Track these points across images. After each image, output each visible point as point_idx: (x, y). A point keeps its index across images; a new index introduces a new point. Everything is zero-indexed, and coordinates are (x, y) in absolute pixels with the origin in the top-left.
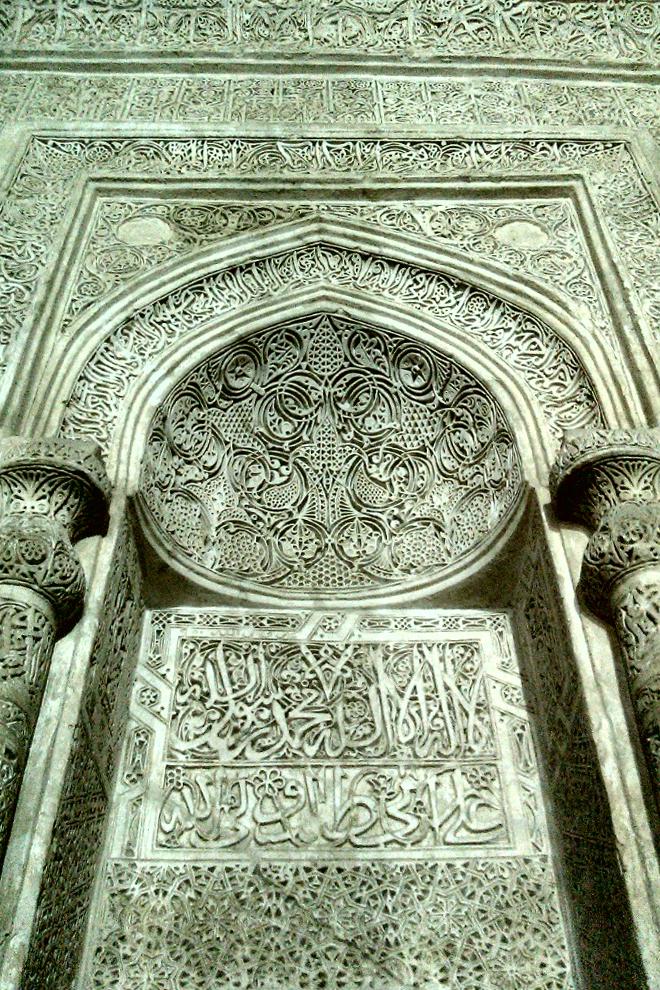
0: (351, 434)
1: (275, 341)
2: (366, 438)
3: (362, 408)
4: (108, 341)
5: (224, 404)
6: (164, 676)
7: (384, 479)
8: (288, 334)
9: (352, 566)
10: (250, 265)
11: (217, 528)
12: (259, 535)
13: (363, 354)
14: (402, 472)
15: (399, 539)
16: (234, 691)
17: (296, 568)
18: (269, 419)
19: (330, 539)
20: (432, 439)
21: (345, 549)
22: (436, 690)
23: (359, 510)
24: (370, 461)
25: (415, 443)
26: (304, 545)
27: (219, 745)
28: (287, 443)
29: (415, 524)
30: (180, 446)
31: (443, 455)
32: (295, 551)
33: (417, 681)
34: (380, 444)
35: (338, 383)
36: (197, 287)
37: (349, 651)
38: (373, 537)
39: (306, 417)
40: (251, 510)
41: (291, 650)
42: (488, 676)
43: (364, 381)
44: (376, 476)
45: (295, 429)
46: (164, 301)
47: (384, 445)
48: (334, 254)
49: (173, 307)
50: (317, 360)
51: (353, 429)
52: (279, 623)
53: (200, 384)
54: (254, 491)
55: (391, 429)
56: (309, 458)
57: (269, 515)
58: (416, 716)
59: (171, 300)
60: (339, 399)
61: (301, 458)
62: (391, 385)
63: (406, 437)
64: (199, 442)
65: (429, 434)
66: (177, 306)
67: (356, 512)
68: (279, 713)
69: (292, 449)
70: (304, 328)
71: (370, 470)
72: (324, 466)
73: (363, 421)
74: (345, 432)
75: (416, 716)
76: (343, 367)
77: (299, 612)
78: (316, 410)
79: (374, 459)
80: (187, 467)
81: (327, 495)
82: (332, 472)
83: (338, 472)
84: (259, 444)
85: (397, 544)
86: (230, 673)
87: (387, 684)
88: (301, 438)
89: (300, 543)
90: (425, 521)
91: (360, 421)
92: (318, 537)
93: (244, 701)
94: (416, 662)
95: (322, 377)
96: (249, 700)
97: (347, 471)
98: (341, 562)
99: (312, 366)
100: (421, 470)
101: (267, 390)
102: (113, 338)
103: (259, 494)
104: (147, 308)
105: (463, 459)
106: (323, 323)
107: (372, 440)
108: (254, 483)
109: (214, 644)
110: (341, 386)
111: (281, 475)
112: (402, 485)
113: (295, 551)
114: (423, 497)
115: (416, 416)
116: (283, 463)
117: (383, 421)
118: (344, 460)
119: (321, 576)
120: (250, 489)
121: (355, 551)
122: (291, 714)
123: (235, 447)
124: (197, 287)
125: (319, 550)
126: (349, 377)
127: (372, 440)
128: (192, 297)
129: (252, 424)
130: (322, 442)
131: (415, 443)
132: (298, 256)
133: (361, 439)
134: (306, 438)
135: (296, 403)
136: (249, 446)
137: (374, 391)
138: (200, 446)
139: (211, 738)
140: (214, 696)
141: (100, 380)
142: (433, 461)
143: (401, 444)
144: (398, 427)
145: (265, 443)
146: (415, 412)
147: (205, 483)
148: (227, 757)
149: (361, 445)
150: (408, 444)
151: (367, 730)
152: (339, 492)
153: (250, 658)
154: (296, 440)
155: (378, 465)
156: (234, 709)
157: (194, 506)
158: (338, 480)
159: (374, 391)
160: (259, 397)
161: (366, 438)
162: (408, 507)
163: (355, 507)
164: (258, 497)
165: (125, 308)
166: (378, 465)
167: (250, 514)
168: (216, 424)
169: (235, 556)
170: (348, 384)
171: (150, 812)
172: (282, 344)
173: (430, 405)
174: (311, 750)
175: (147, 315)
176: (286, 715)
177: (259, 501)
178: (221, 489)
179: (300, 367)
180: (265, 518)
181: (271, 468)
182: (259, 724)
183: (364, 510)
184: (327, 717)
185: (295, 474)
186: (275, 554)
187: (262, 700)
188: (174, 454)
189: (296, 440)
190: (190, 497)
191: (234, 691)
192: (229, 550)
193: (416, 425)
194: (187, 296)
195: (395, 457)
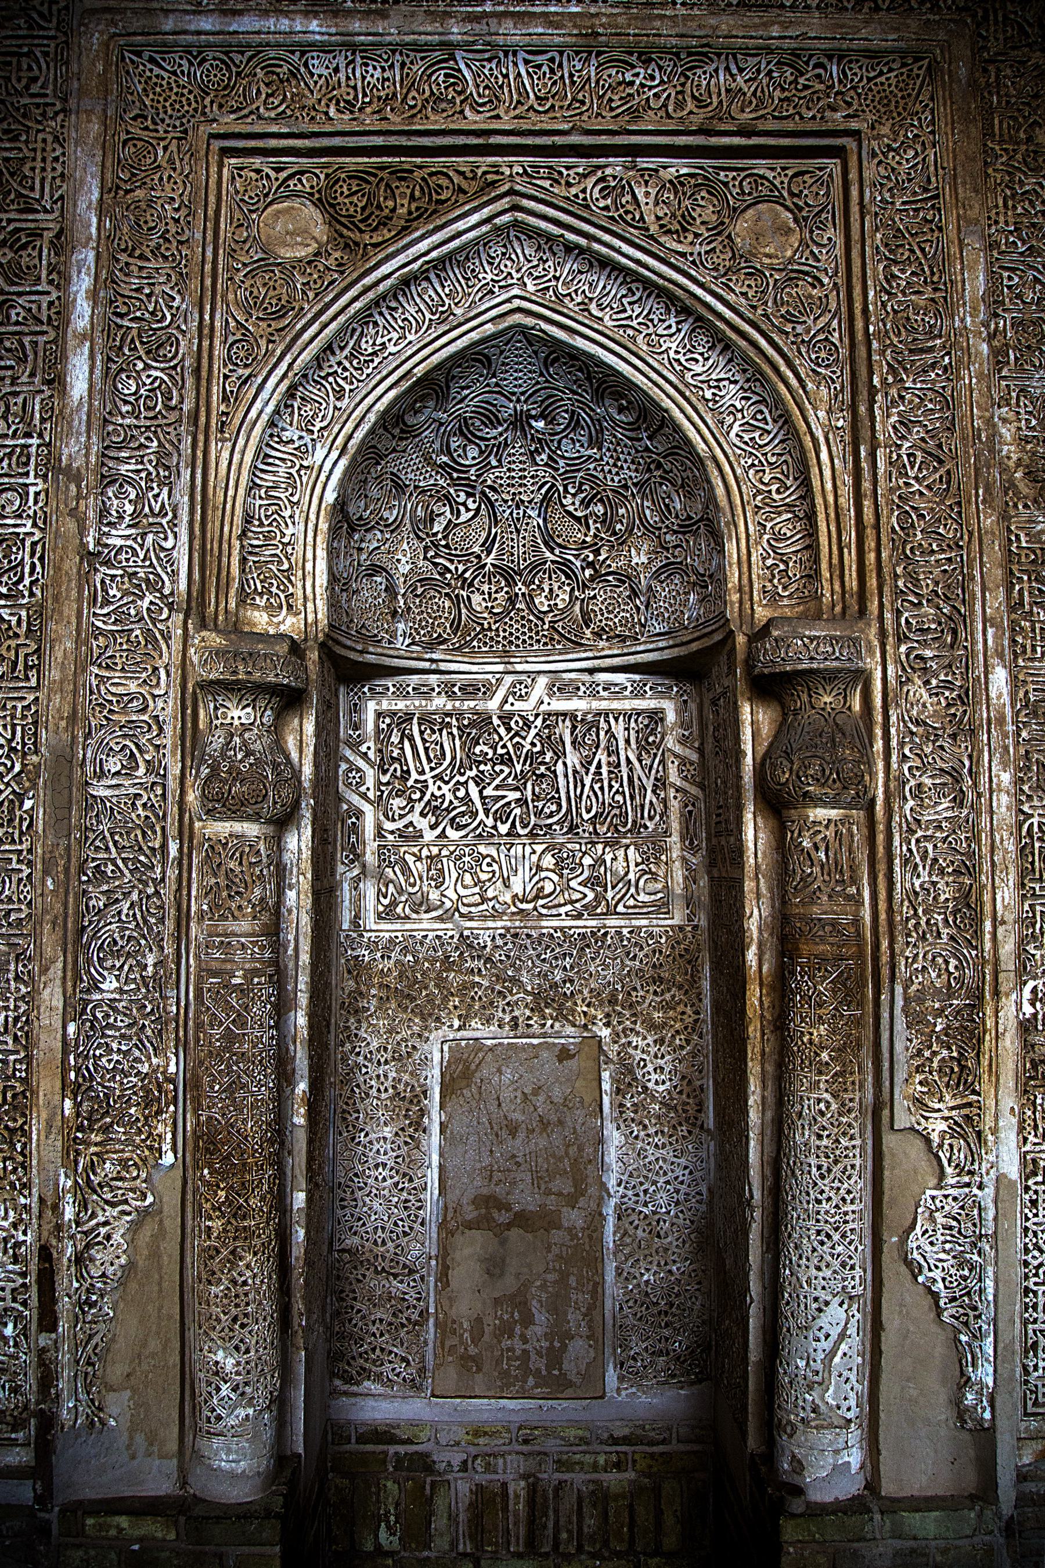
2: (561, 463)
6: (366, 754)
7: (579, 514)
16: (432, 769)
17: (486, 626)
18: (453, 446)
22: (619, 765)
24: (566, 491)
26: (494, 596)
27: (422, 824)
32: (484, 604)
33: (602, 756)
34: (578, 471)
35: (531, 400)
37: (539, 722)
41: (483, 721)
42: (669, 750)
43: (562, 399)
44: (571, 508)
47: (581, 474)
48: (530, 238)
52: (470, 690)
54: (440, 536)
58: (599, 793)
67: (548, 554)
68: (474, 791)
71: (564, 501)
75: (599, 793)
77: (489, 676)
86: (426, 749)
87: (572, 758)
92: (508, 585)
93: (442, 779)
94: (602, 733)
96: (447, 779)
103: (445, 537)
107: (568, 465)
109: (408, 717)
113: (484, 604)
119: (511, 634)
120: (435, 534)
122: (485, 793)
127: (568, 465)
135: (483, 423)
136: (432, 482)
139: (415, 817)
140: (414, 776)
148: (429, 836)
151: (554, 808)
153: (445, 732)
155: (574, 495)
156: (432, 788)
161: (561, 463)
163: (546, 543)
166: (574, 495)
170: (542, 402)
171: (369, 889)
174: (504, 829)
176: (481, 792)
180: (452, 568)
182: (456, 803)
184: (517, 795)
187: (458, 778)
191: (432, 769)
195: (592, 488)
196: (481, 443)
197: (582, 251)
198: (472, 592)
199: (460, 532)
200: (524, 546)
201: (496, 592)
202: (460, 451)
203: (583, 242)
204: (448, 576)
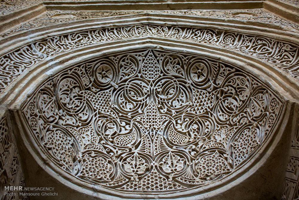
0: (166, 110)
7: (184, 131)
9: (168, 178)
11: (83, 153)
12: (110, 160)
14: (195, 126)
15: (197, 162)
17: (132, 179)
19: (154, 163)
20: (211, 107)
21: (164, 169)
23: (171, 147)
24: (177, 123)
25: (202, 111)
26: (138, 166)
28: (130, 114)
29: (206, 152)
30: (65, 105)
31: (219, 114)
34: (182, 114)
38: (181, 161)
40: (106, 146)
44: (181, 130)
45: (135, 107)
47: (184, 114)
51: (166, 107)
54: (109, 136)
55: (187, 106)
56: (142, 122)
57: (117, 149)
61: (137, 122)
63: (196, 108)
64: (77, 106)
65: (209, 105)
67: (169, 149)
69: (132, 117)
71: (176, 127)
72: (150, 125)
73: (172, 103)
74: (162, 109)
79: (179, 122)
80: (68, 117)
82: (155, 128)
83: (159, 129)
85: (196, 164)
88: (138, 112)
89: (136, 166)
90: (212, 150)
91: (170, 103)
97: (163, 128)
98: (161, 176)
103: (113, 138)
105: (231, 113)
108: (110, 132)
111: (126, 130)
112: (196, 133)
113: (132, 169)
114: (209, 138)
115: (201, 97)
116: (127, 124)
117: (183, 102)
118: (161, 123)
121: (170, 169)
123: (99, 113)
125: (147, 170)
127: (177, 112)
131: (202, 111)
133: (171, 111)
134: (140, 112)
136: (108, 113)
142: (213, 118)
143: (194, 113)
144: (191, 104)
145: (118, 114)
146: (200, 95)
147: (79, 128)
149: (171, 115)
150: (198, 112)
154: (135, 113)
155: (181, 124)
157: (69, 138)
158: (158, 132)
161: (173, 111)
162: (200, 144)
164: (111, 140)
166: (181, 124)
167: (105, 148)
168: (89, 99)
169: (93, 170)
173: (209, 90)
177: (112, 142)
178: (89, 133)
180: (115, 151)
181: (120, 126)
183: (174, 147)
185: (134, 129)
186: (119, 170)
188: (59, 108)
189: (135, 113)
190: (67, 133)
192: (89, 166)
193: (201, 102)
195: (190, 120)
198: (126, 163)
199: (122, 137)
200: (156, 146)
201: (140, 165)
202: (124, 104)
204: (112, 154)
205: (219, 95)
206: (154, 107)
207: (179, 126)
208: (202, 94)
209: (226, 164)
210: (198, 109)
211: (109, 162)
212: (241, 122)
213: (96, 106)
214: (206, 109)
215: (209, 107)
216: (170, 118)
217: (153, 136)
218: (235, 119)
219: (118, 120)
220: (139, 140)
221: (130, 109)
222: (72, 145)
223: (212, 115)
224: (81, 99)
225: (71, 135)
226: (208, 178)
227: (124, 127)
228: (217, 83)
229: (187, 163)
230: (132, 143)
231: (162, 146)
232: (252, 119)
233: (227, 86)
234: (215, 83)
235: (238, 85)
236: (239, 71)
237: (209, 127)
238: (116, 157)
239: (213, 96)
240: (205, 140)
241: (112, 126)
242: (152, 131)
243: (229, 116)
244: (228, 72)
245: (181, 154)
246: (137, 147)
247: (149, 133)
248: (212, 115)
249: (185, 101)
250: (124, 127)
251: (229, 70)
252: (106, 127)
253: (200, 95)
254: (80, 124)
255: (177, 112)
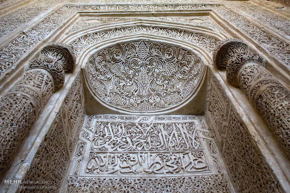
0: (151, 74)
1: (127, 47)
3: (154, 66)
4: (79, 39)
5: (112, 62)
8: (131, 45)
10: (121, 29)
11: (110, 93)
13: (154, 51)
14: (167, 82)
15: (166, 98)
17: (134, 105)
18: (126, 69)
20: (175, 72)
23: (154, 92)
24: (157, 80)
28: (131, 76)
30: (99, 69)
34: (160, 76)
36: (106, 32)
39: (137, 69)
44: (159, 84)
46: (96, 33)
47: (161, 76)
48: (145, 28)
49: (98, 35)
50: (140, 53)
51: (151, 72)
53: (106, 54)
55: (163, 71)
57: (126, 92)
59: (98, 34)
60: (147, 64)
61: (136, 80)
62: (162, 59)
63: (167, 73)
64: (105, 71)
65: (174, 70)
66: (100, 35)
69: (133, 77)
70: (136, 44)
74: (149, 73)
76: (148, 56)
78: (140, 67)
79: (158, 80)
80: (101, 75)
81: (144, 89)
82: (145, 83)
83: (147, 83)
84: (123, 75)
88: (136, 75)
89: (136, 100)
90: (174, 92)
91: (153, 70)
95: (142, 58)
99: (139, 55)
100: (172, 80)
101: (125, 61)
102: (81, 39)
104: (91, 34)
105: (185, 74)
106: (142, 43)
108: (122, 84)
110: (148, 61)
111: (130, 83)
112: (167, 85)
114: (173, 87)
115: (170, 66)
116: (130, 81)
117: (160, 69)
118: (149, 80)
123: (116, 75)
124: (106, 32)
126: (150, 58)
127: (157, 75)
128: (104, 34)
129: (121, 70)
130: (142, 76)
132: (135, 28)
134: (137, 75)
136: (120, 75)
137: (157, 62)
138: (105, 72)
141: (76, 47)
142: (176, 77)
143: (166, 75)
144: (165, 70)
145: (125, 75)
146: (170, 65)
149: (154, 76)
150: (168, 74)
152: (147, 88)
154: (134, 75)
155: (159, 81)
157: (102, 85)
158: (147, 85)
159: (157, 62)
160: (123, 63)
161: (155, 74)
164: (122, 88)
165: (85, 33)
166: (159, 81)
167: (120, 91)
168: (110, 67)
170: (149, 60)
172: (130, 48)
173: (174, 62)
175: (91, 36)
177: (123, 89)
178: (111, 84)
179: (135, 55)
180: (125, 93)
188: (97, 71)
189: (134, 75)
193: (170, 69)
194: (103, 34)
196: (134, 70)
197: (156, 27)
199: (128, 87)
202: (128, 71)
203: (157, 25)
204: (123, 94)
205: (179, 65)
206: (145, 72)
207: (158, 82)
208: (171, 65)
209: (180, 97)
210: (168, 73)
211: (122, 98)
212: (189, 78)
213: (114, 71)
214: (173, 73)
215: (174, 72)
216: (153, 78)
217: (144, 87)
218: (186, 77)
219: (126, 79)
220: (137, 88)
221: (132, 73)
222: (104, 88)
223: (175, 75)
224: (106, 67)
225: (103, 84)
226: (171, 104)
227: (129, 82)
228: (179, 59)
229: (162, 98)
230: (134, 89)
231: (149, 91)
232: (194, 76)
233: (183, 60)
234: (177, 59)
235: (189, 59)
236: (189, 52)
237: (174, 82)
238: (125, 96)
239: (176, 66)
240: (171, 88)
241: (123, 82)
242: (144, 84)
243: (184, 75)
244: (184, 53)
245: (159, 95)
246: (136, 92)
247: (142, 85)
248: (175, 75)
249: (161, 69)
250: (129, 82)
251: (184, 52)
252: (119, 82)
253: (170, 65)
254: (107, 80)
255: (157, 75)
